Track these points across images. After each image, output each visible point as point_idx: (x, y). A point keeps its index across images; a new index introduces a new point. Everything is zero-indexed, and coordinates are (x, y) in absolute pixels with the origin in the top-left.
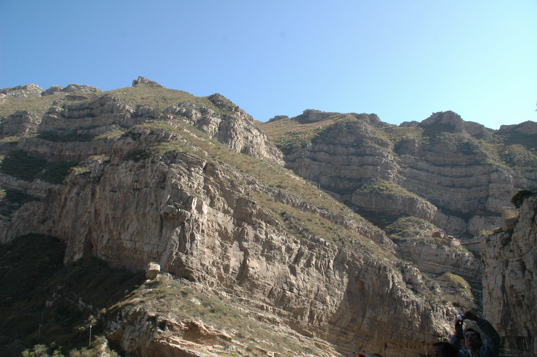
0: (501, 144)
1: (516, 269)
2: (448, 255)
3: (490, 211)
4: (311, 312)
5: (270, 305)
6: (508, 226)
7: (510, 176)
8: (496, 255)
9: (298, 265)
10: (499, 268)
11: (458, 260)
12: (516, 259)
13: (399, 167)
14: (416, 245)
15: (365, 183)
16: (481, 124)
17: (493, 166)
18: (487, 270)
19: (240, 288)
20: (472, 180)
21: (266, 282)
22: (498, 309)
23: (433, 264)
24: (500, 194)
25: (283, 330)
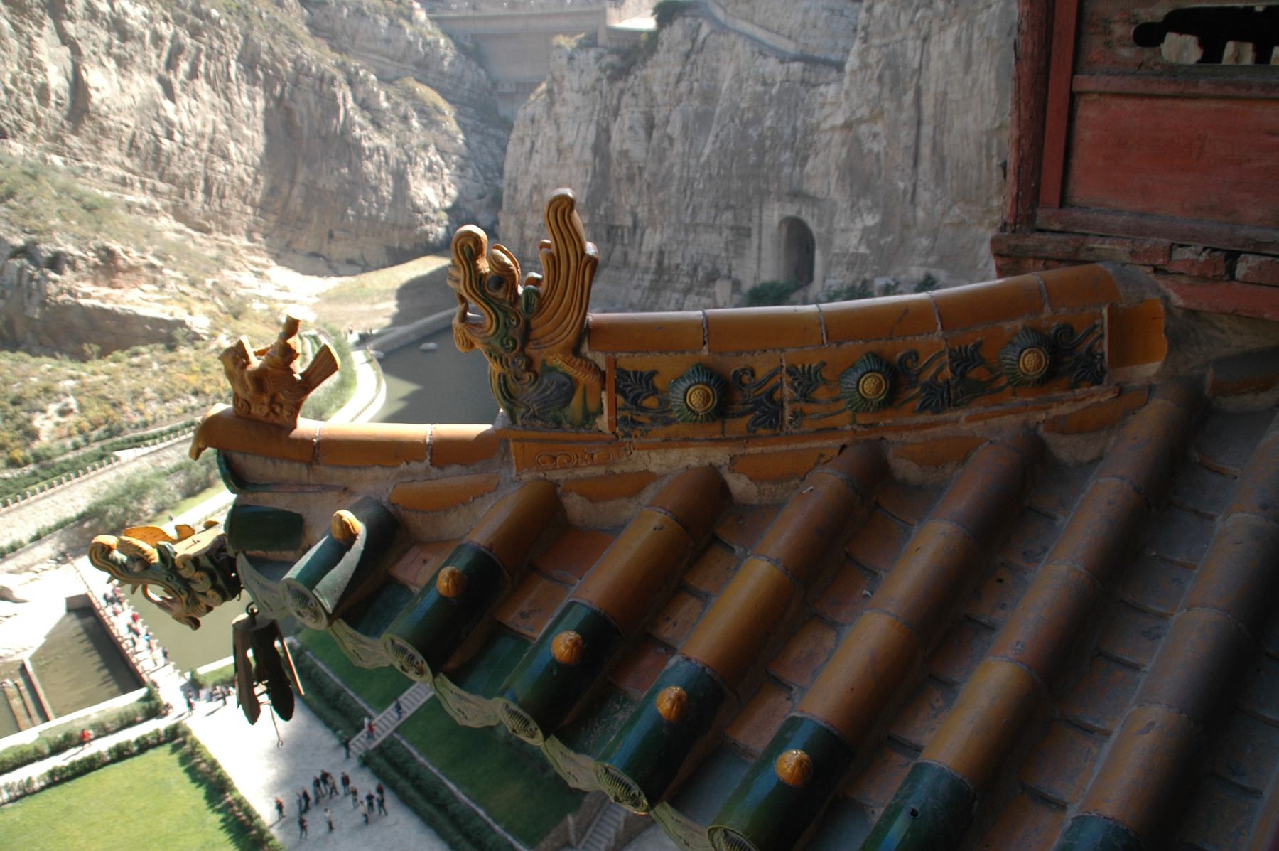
2: (409, 43)
4: (207, 180)
5: (133, 173)
9: (176, 76)
11: (427, 55)
12: (641, 109)
14: (348, 16)
19: (75, 138)
21: (124, 121)
25: (167, 225)
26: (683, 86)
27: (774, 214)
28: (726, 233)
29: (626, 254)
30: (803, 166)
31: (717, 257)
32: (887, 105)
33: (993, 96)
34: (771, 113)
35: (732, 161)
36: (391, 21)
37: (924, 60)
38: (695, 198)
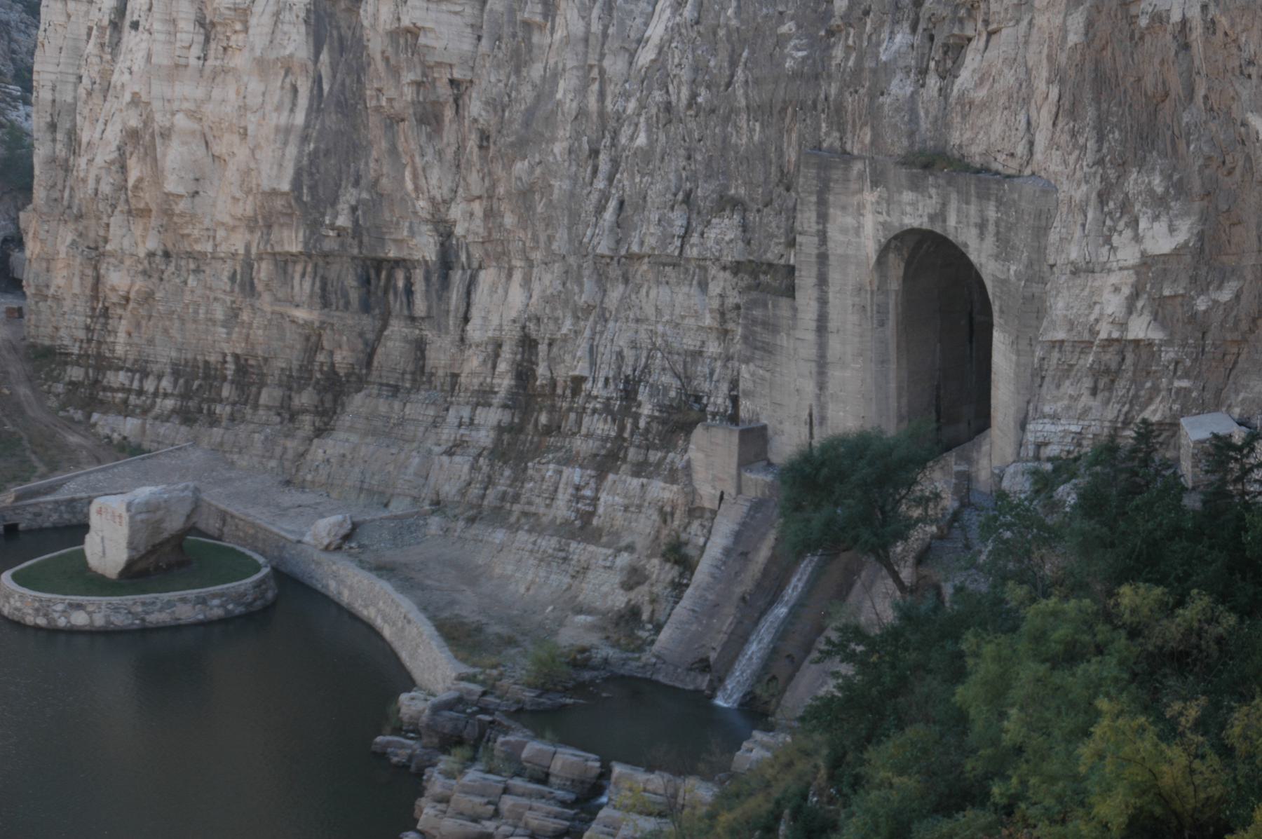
28: (720, 282)
29: (420, 346)
30: (948, 75)
35: (733, 64)
38: (622, 177)
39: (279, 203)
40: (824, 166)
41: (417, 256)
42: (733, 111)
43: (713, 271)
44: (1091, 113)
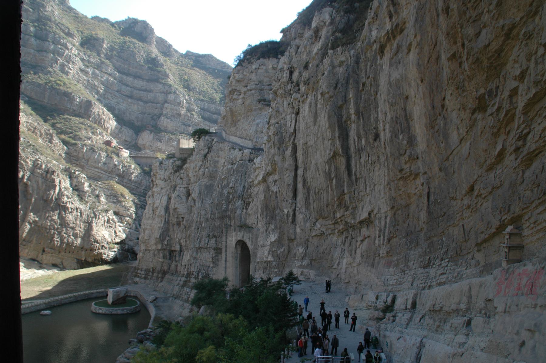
0: (183, 68)
1: (182, 195)
2: (115, 165)
3: (160, 129)
6: (181, 154)
7: (184, 101)
8: (166, 177)
10: (166, 189)
13: (81, 64)
15: (40, 71)
16: (171, 43)
17: (172, 88)
18: (155, 189)
20: (150, 96)
22: (159, 225)
23: (100, 171)
24: (172, 115)
26: (202, 170)
27: (232, 239)
28: (212, 252)
30: (247, 209)
31: (209, 266)
32: (277, 158)
33: (329, 134)
34: (233, 179)
36: (108, 155)
37: (297, 127)
39: (158, 240)
40: (227, 228)
41: (177, 249)
42: (216, 219)
43: (211, 250)
44: (265, 213)
